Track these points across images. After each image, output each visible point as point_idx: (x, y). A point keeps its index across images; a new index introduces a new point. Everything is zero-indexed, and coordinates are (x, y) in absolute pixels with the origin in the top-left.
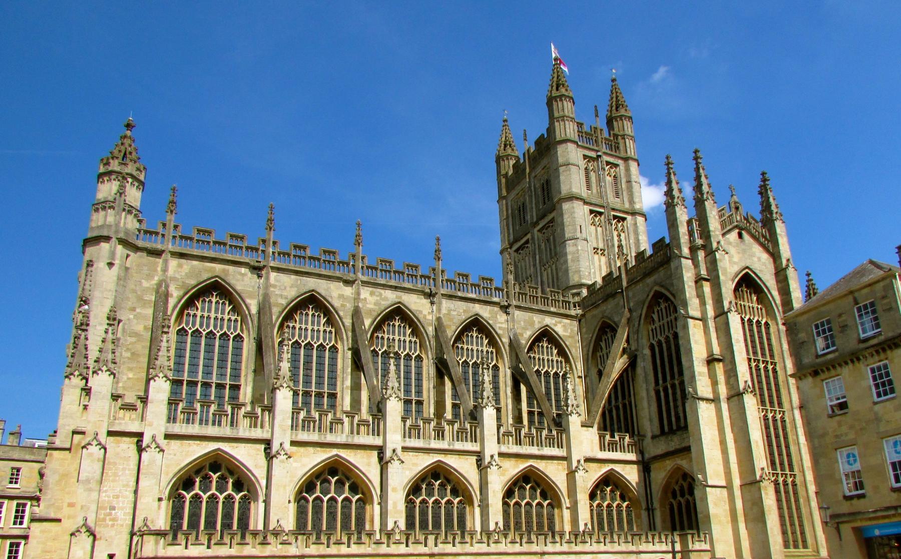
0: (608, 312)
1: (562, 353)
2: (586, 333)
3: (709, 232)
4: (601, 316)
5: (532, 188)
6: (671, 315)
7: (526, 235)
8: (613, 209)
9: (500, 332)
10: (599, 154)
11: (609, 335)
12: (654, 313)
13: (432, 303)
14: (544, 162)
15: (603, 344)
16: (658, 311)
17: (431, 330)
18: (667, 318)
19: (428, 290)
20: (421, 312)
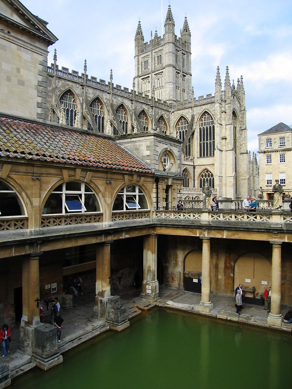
0: (184, 113)
1: (165, 124)
2: (173, 118)
3: (229, 97)
4: (181, 114)
5: (153, 57)
6: (209, 120)
7: (148, 74)
8: (183, 72)
9: (150, 116)
10: (180, 49)
11: (183, 121)
12: (203, 118)
13: (132, 103)
14: (161, 48)
15: (180, 124)
16: (204, 118)
17: (131, 113)
18: (208, 120)
19: (130, 99)
20: (129, 106)
